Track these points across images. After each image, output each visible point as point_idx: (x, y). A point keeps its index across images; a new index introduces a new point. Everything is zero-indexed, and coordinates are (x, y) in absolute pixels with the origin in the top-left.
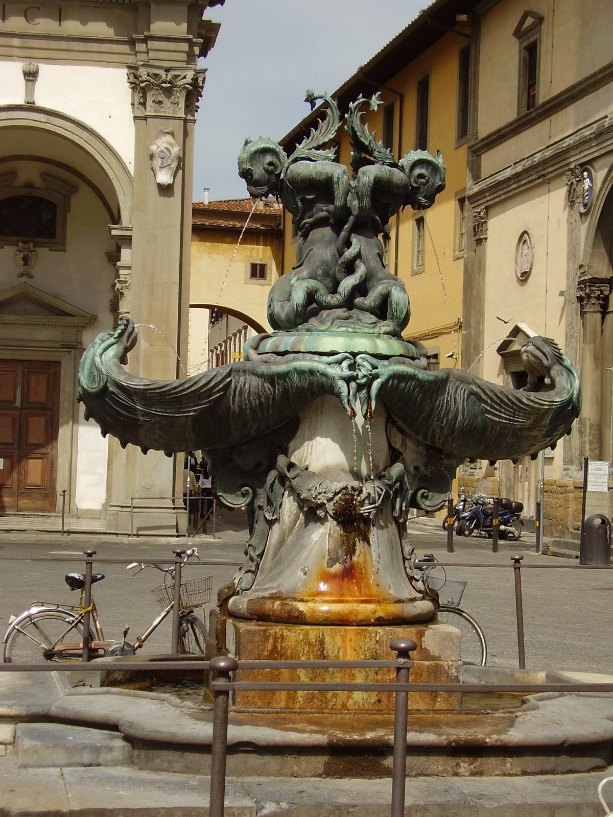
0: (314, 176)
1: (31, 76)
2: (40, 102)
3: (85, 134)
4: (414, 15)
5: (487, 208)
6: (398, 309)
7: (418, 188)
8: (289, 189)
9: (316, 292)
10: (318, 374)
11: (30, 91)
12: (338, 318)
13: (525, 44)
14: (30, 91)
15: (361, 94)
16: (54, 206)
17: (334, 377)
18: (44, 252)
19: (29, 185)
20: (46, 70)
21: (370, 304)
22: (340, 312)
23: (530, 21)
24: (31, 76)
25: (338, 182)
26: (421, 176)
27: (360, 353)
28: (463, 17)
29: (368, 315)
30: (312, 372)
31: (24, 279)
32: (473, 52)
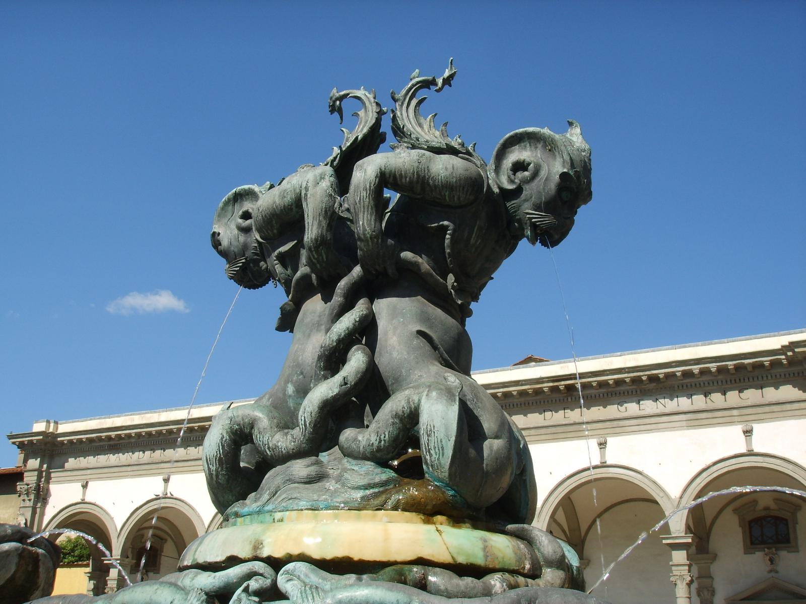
1: (748, 433)
2: (757, 449)
3: (791, 466)
6: (432, 445)
7: (518, 191)
9: (252, 427)
11: (749, 443)
12: (291, 481)
14: (749, 443)
15: (417, 71)
16: (786, 520)
18: (783, 554)
19: (767, 509)
20: (757, 428)
21: (368, 439)
22: (300, 468)
24: (748, 433)
26: (519, 166)
27: (290, 559)
29: (369, 466)
31: (773, 574)
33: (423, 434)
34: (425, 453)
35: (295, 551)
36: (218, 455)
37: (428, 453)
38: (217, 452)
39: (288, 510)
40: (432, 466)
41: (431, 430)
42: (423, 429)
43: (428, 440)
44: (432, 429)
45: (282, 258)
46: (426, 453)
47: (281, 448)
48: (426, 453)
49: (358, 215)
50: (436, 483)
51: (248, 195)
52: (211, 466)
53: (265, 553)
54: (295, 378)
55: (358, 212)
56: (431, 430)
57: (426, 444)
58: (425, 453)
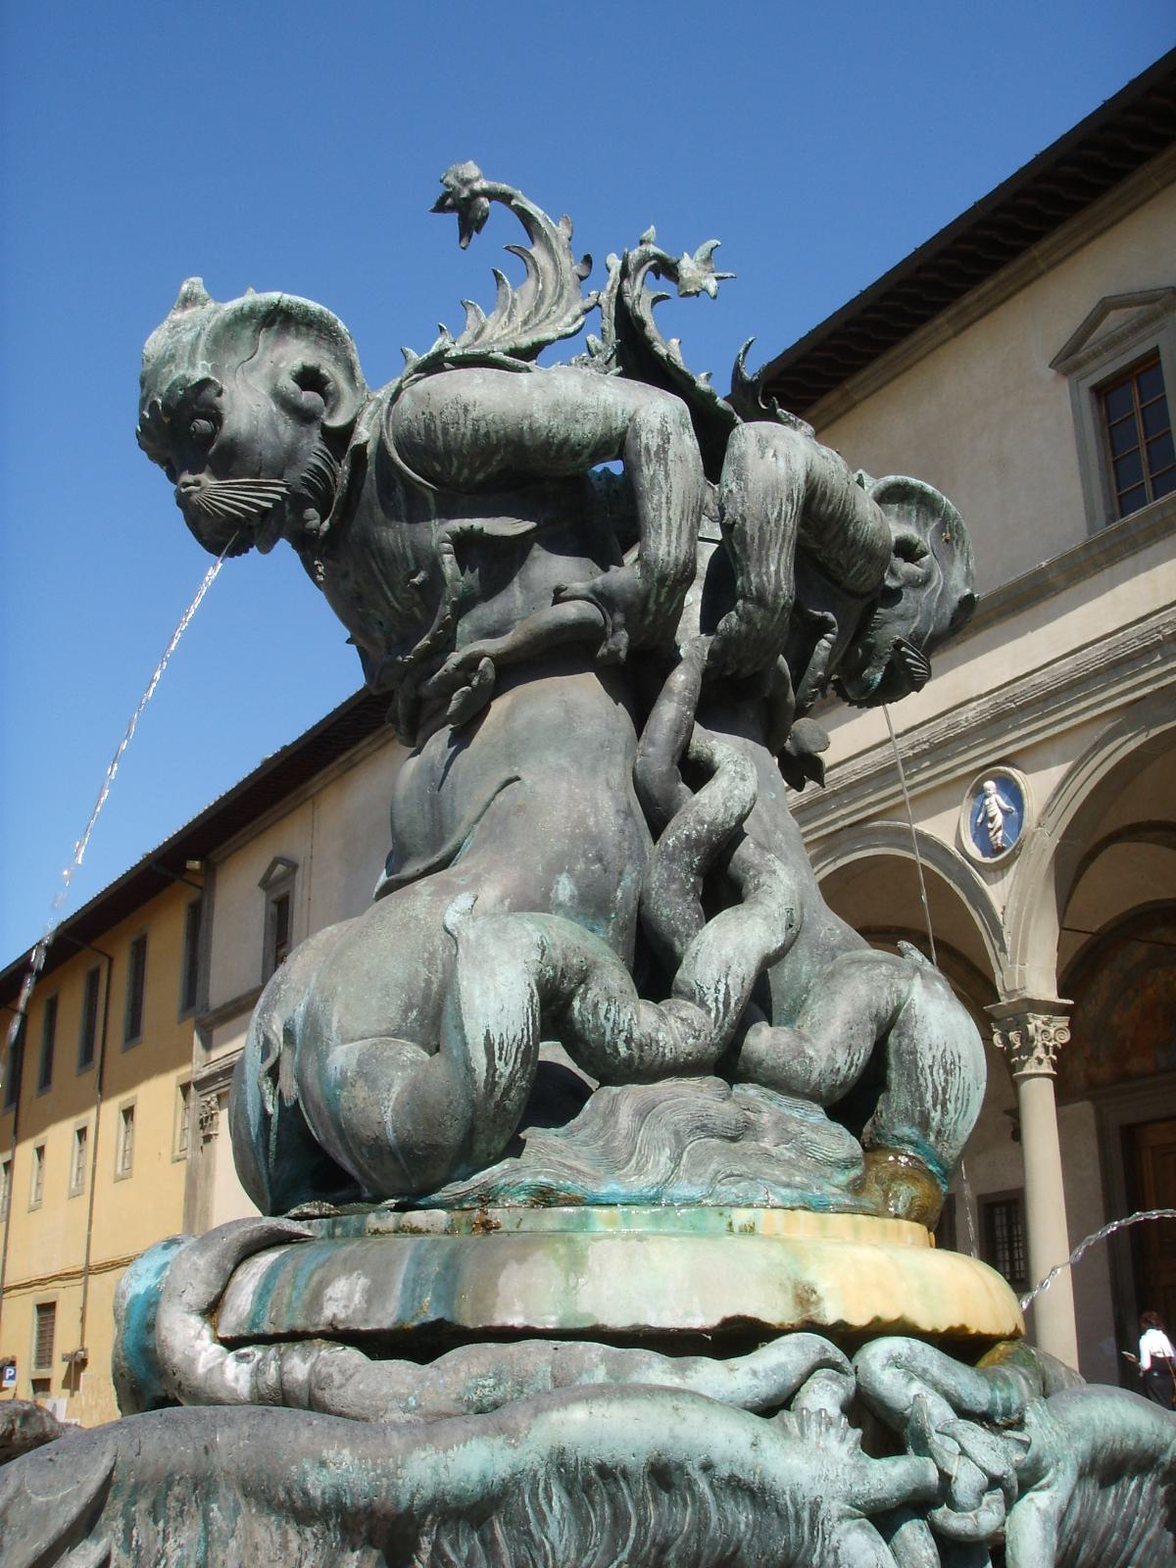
0: (542, 418)
4: (135, 859)
5: (218, 1096)
6: (952, 1093)
8: (399, 493)
9: (584, 977)
10: (703, 1486)
13: (274, 896)
17: (816, 1506)
21: (831, 1059)
23: (280, 868)
25: (663, 450)
27: (879, 1329)
28: (195, 865)
30: (664, 1475)
32: (205, 905)
33: (931, 1067)
34: (929, 1104)
35: (890, 1314)
36: (525, 1040)
37: (939, 1107)
38: (523, 1030)
39: (750, 1206)
40: (939, 1133)
41: (953, 1063)
42: (929, 1056)
43: (946, 1081)
44: (957, 1060)
45: (467, 546)
46: (934, 1106)
47: (664, 1048)
48: (934, 1106)
49: (768, 549)
50: (930, 1167)
51: (310, 325)
52: (499, 1064)
53: (830, 1315)
54: (580, 866)
55: (770, 541)
56: (953, 1063)
57: (940, 1088)
58: (929, 1104)
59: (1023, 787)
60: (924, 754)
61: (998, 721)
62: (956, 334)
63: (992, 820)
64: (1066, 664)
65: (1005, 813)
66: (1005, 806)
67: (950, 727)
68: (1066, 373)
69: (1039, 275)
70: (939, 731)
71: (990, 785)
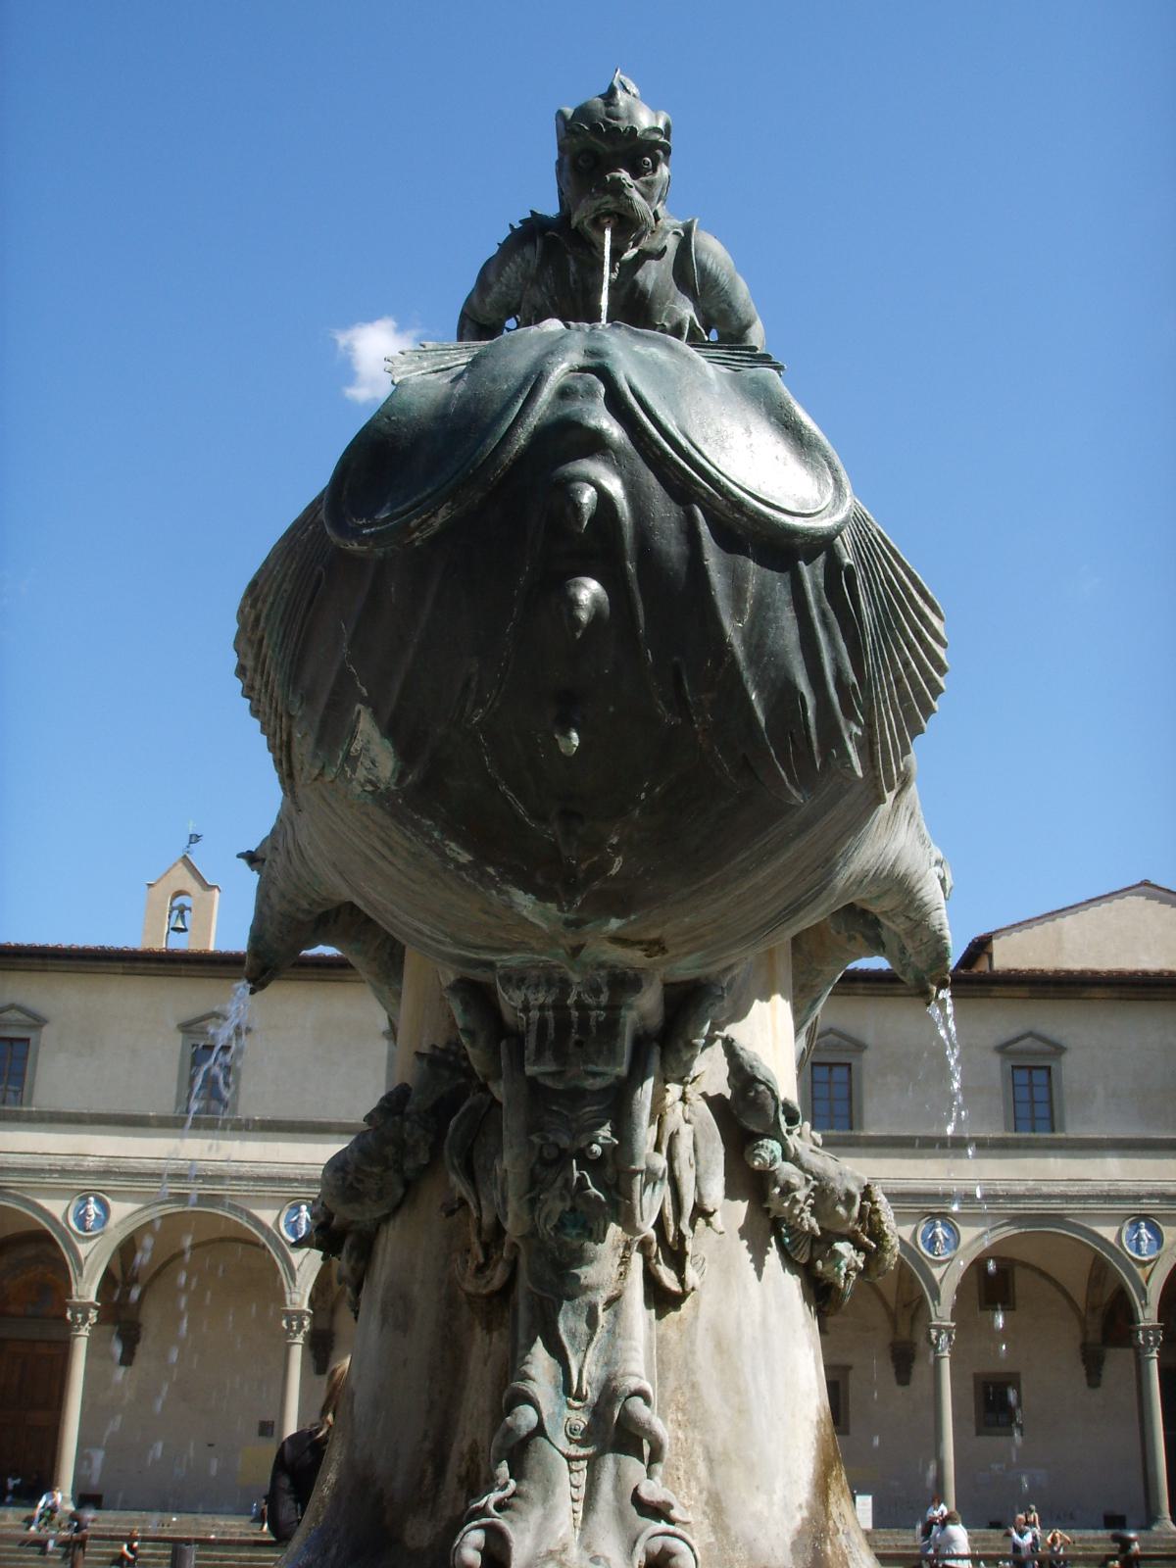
59: (111, 1208)
60: (57, 1171)
61: (106, 1173)
62: (123, 974)
63: (90, 1216)
64: (151, 1163)
65: (97, 1215)
66: (98, 1212)
67: (76, 1165)
68: (183, 1031)
69: (180, 976)
70: (71, 1163)
71: (92, 1199)
